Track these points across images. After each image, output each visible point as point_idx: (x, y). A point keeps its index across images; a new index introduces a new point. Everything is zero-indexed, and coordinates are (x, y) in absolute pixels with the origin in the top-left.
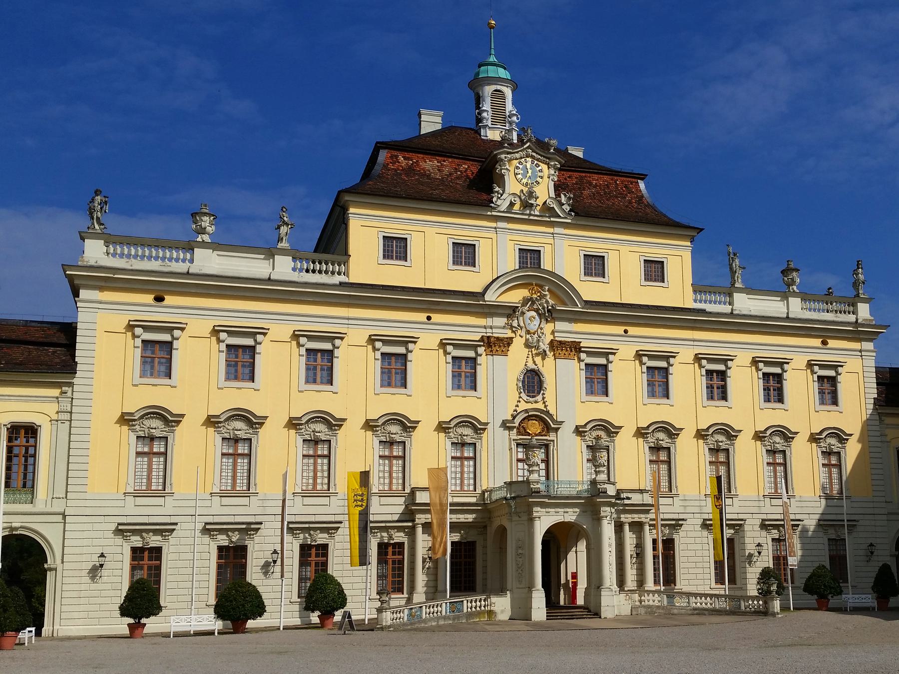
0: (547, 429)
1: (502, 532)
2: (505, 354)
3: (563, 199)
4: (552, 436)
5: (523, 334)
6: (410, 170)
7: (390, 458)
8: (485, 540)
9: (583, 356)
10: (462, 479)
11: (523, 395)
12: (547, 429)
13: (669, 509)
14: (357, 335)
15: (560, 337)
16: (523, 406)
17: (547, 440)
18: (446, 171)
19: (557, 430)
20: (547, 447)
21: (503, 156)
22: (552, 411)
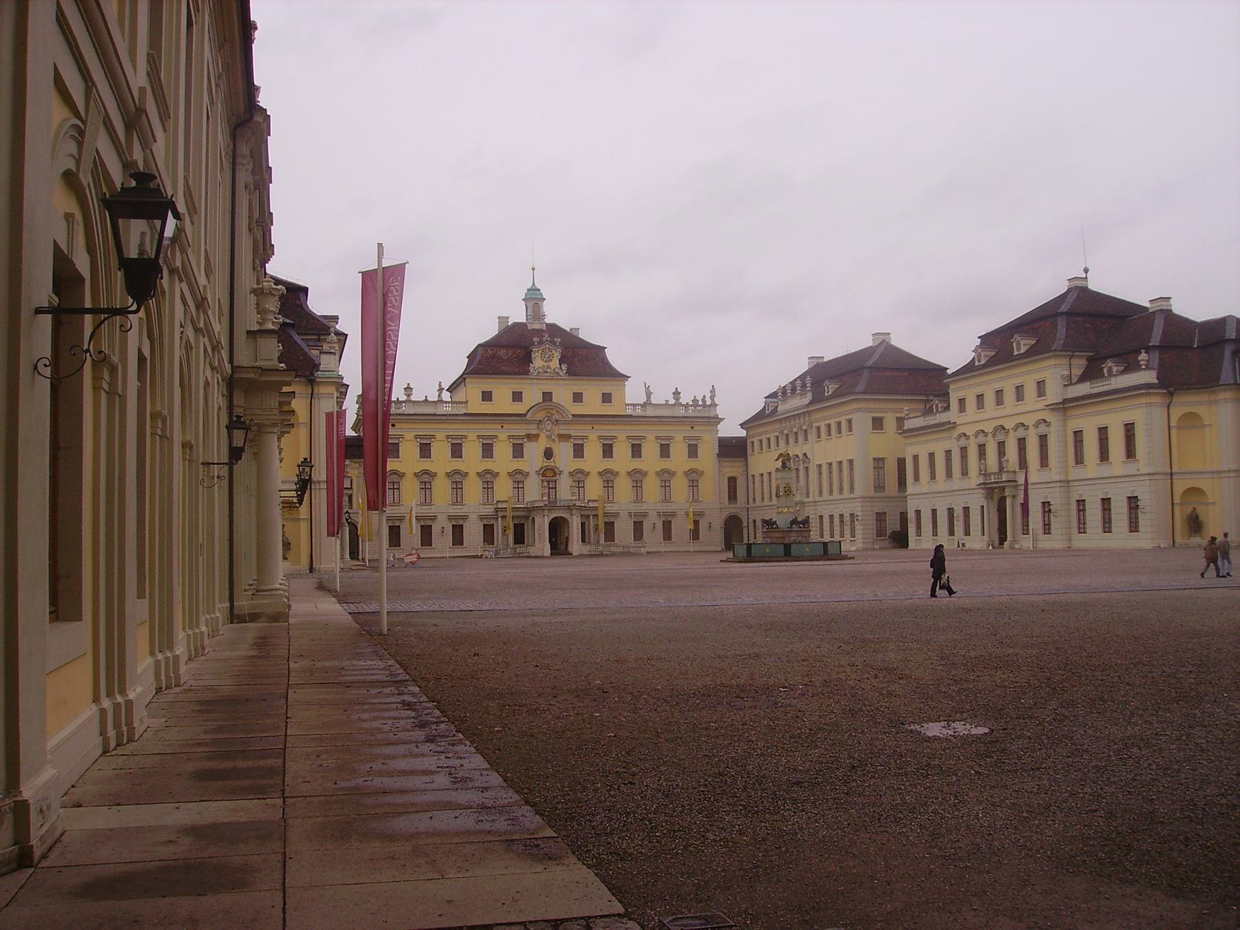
0: (555, 474)
1: (534, 519)
2: (537, 441)
3: (564, 367)
4: (558, 477)
5: (544, 431)
6: (493, 357)
7: (488, 488)
8: (528, 523)
9: (572, 440)
10: (518, 496)
12: (555, 474)
13: (611, 508)
14: (472, 436)
15: (562, 432)
18: (510, 354)
19: (560, 474)
20: (555, 482)
21: (534, 349)
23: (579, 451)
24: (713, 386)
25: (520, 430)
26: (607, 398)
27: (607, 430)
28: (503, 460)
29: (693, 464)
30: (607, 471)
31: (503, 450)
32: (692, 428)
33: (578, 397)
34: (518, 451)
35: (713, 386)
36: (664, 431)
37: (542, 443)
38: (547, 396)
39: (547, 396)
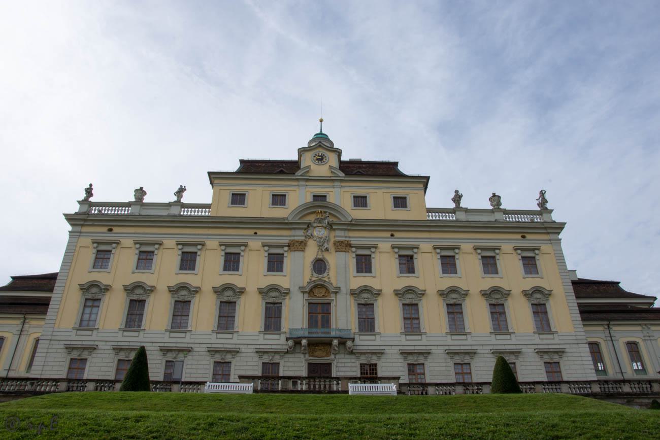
4: (333, 297)
9: (354, 249)
11: (314, 274)
16: (314, 279)
17: (330, 300)
19: (336, 293)
22: (333, 281)
23: (364, 264)
26: (400, 202)
27: (405, 238)
32: (523, 237)
33: (360, 201)
34: (275, 263)
37: (311, 252)
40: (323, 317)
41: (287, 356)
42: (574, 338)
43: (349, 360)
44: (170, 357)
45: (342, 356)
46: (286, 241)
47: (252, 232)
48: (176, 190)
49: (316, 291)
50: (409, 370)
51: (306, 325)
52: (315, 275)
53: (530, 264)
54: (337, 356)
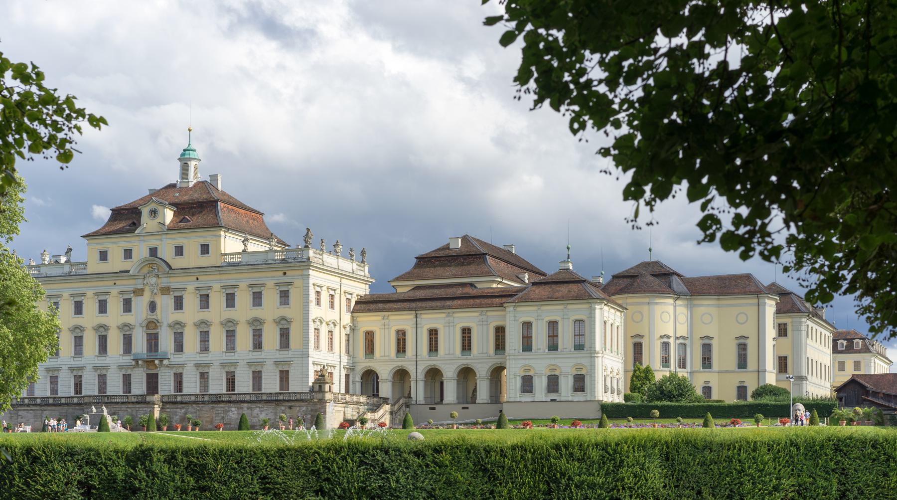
12: (156, 327)
16: (149, 317)
23: (179, 304)
24: (308, 230)
25: (128, 285)
26: (205, 249)
28: (115, 316)
29: (285, 312)
30: (204, 322)
31: (115, 306)
32: (285, 274)
33: (179, 251)
34: (127, 306)
35: (308, 230)
36: (256, 277)
37: (146, 298)
38: (153, 251)
39: (153, 251)
40: (155, 342)
41: (134, 369)
42: (301, 353)
43: (167, 371)
44: (75, 373)
45: (163, 369)
46: (131, 288)
47: (112, 283)
48: (66, 250)
49: (150, 325)
50: (201, 376)
51: (145, 351)
52: (149, 313)
53: (285, 296)
54: (161, 369)
